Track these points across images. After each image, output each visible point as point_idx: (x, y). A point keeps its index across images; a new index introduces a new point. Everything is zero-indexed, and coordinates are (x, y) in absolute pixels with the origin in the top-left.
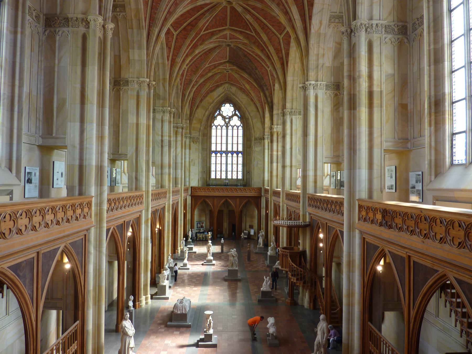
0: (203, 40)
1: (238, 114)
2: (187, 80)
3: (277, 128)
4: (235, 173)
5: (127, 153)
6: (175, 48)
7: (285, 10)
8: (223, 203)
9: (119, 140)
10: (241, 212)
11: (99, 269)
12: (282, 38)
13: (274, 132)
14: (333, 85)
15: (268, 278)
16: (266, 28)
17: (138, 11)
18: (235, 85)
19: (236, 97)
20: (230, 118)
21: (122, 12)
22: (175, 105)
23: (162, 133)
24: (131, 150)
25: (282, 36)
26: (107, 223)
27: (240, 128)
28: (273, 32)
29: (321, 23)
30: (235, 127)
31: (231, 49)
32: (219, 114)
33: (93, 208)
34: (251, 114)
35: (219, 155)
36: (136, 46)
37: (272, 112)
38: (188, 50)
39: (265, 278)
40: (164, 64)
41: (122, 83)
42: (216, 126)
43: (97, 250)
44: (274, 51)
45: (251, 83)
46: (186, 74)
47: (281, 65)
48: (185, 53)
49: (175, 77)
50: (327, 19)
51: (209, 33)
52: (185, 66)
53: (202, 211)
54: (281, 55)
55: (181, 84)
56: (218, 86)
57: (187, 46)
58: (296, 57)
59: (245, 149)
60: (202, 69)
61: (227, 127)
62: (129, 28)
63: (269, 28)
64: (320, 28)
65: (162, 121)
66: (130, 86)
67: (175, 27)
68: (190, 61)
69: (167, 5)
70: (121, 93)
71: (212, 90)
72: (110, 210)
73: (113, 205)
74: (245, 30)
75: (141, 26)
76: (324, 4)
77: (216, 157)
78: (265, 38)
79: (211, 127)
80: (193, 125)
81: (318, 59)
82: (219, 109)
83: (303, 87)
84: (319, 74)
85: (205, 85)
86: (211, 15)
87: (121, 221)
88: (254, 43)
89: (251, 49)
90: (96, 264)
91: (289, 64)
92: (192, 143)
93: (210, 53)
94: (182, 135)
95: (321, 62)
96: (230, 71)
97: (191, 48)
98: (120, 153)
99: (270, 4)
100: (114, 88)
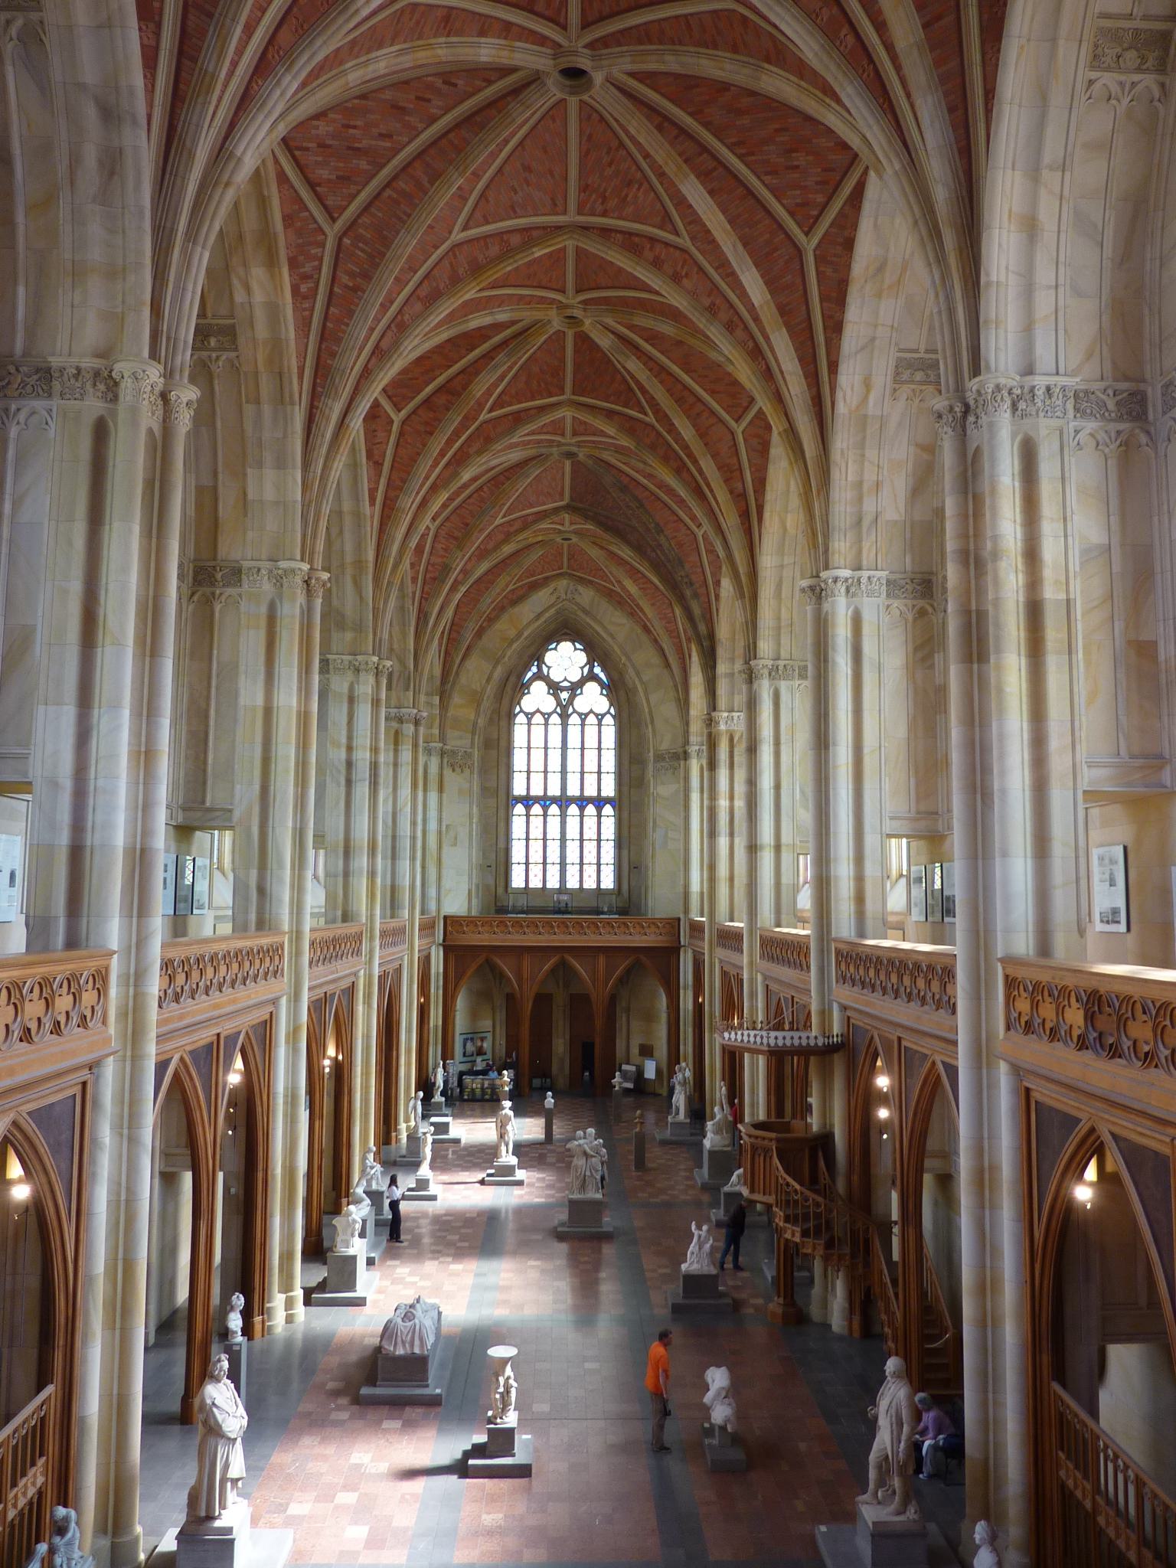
0: (485, 438)
1: (602, 676)
2: (433, 565)
3: (733, 722)
4: (590, 871)
5: (231, 804)
6: (396, 465)
7: (751, 344)
8: (553, 971)
9: (205, 762)
10: (613, 999)
11: (127, 1201)
13: (719, 734)
14: (912, 580)
15: (705, 1228)
17: (276, 345)
18: (591, 582)
19: (594, 618)
20: (575, 688)
21: (225, 350)
22: (396, 646)
23: (350, 738)
24: (244, 795)
25: (744, 424)
26: (158, 1043)
27: (609, 720)
28: (713, 413)
29: (867, 384)
30: (591, 716)
31: (577, 467)
32: (539, 676)
33: (113, 991)
35: (537, 809)
36: (268, 457)
37: (714, 667)
38: (438, 470)
39: (693, 1227)
40: (357, 515)
41: (219, 576)
42: (526, 714)
43: (121, 1135)
45: (644, 576)
48: (427, 478)
50: (889, 373)
51: (505, 416)
52: (426, 521)
53: (482, 998)
54: (739, 485)
55: (414, 580)
56: (534, 587)
58: (788, 491)
59: (625, 789)
60: (482, 530)
61: (564, 717)
62: (247, 402)
63: (699, 400)
64: (866, 398)
65: (351, 700)
66: (245, 586)
68: (444, 506)
69: (372, 330)
70: (218, 608)
71: (516, 599)
72: (172, 996)
73: (180, 979)
74: (626, 406)
75: (287, 395)
76: (876, 326)
77: (528, 816)
78: (687, 432)
79: (511, 717)
81: (860, 499)
82: (538, 660)
83: (812, 588)
84: (866, 545)
85: (492, 582)
86: (513, 360)
87: (206, 1036)
88: (653, 447)
89: (641, 466)
90: (120, 1184)
91: (767, 515)
92: (447, 772)
93: (508, 479)
94: (415, 746)
95: (869, 506)
96: (575, 539)
98: (208, 804)
99: (701, 326)
100: (193, 594)
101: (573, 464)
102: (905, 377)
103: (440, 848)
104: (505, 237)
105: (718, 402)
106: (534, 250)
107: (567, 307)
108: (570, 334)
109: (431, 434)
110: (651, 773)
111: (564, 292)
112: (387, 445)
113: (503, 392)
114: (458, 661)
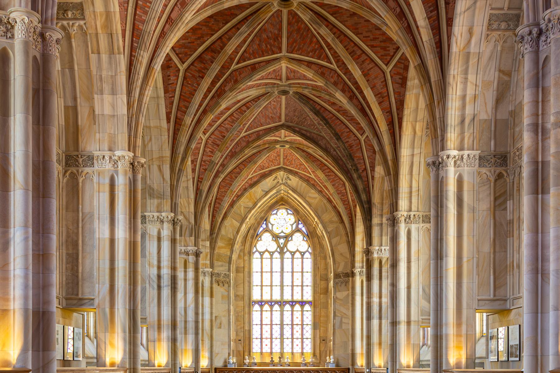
6: (182, 97)
12: (390, 72)
13: (373, 259)
16: (359, 52)
27: (307, 255)
28: (372, 60)
34: (328, 228)
37: (370, 220)
38: (207, 101)
44: (374, 99)
46: (204, 151)
47: (388, 125)
49: (183, 155)
50: (485, 24)
52: (200, 134)
58: (417, 108)
61: (282, 253)
63: (364, 52)
68: (210, 125)
80: (216, 251)
86: (251, 30)
88: (335, 84)
89: (327, 97)
91: (404, 124)
94: (197, 269)
97: (213, 97)
101: (286, 98)
102: (495, 26)
103: (212, 329)
105: (374, 53)
108: (285, 12)
109: (203, 78)
110: (332, 285)
112: (177, 84)
113: (245, 51)
114: (220, 220)
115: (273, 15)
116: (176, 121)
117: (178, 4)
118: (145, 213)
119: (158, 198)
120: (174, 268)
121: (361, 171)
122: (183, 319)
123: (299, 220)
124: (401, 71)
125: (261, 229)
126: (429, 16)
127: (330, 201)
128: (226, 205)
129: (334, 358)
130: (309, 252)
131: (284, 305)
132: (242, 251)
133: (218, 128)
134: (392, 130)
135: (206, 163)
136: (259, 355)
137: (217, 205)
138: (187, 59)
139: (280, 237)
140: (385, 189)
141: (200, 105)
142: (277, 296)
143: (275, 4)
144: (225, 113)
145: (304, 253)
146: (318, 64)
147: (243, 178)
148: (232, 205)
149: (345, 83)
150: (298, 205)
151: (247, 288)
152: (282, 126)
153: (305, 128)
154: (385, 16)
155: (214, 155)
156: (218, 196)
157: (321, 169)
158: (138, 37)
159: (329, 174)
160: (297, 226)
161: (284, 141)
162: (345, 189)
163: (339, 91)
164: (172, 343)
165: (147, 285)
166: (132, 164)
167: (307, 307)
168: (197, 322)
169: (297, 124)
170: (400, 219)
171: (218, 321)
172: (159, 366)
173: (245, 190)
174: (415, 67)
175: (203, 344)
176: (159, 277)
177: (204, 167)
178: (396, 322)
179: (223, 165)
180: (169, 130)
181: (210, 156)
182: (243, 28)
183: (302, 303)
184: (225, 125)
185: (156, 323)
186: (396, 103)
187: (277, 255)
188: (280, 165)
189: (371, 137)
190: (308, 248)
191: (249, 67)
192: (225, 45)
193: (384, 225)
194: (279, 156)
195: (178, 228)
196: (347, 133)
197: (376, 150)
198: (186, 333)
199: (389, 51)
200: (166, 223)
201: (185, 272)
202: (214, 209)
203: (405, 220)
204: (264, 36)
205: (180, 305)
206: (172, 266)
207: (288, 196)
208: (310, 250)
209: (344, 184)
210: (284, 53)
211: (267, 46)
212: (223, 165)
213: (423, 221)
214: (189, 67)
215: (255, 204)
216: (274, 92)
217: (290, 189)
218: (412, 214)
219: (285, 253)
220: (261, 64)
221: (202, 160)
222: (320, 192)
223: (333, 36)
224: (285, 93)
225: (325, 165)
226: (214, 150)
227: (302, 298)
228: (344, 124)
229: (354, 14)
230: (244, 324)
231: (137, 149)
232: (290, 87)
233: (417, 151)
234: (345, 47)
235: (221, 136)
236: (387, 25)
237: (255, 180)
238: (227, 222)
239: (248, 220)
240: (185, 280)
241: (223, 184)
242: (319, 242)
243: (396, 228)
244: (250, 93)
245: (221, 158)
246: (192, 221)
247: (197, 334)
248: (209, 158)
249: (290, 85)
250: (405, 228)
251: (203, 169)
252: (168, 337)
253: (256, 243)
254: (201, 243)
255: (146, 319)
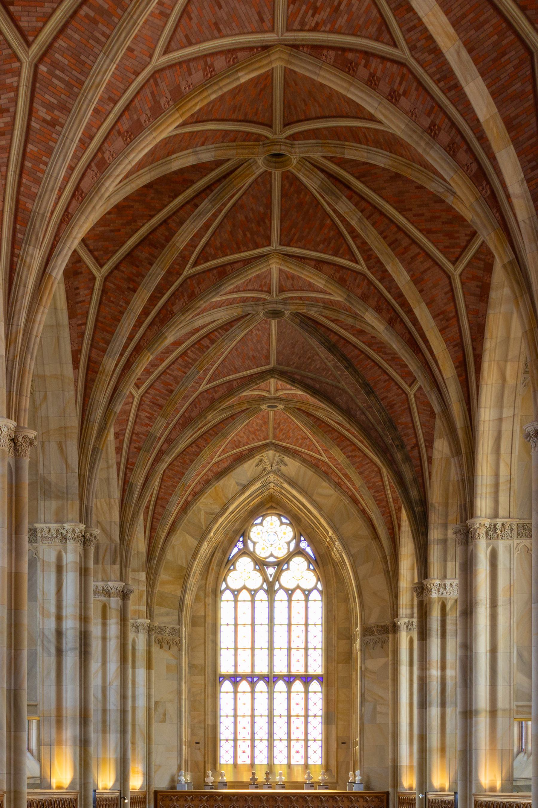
6: (99, 324)
12: (460, 275)
13: (430, 602)
27: (315, 595)
28: (428, 256)
34: (351, 549)
37: (426, 534)
44: (433, 323)
46: (137, 416)
47: (456, 368)
49: (100, 424)
52: (130, 388)
57: (139, 318)
58: (508, 337)
61: (271, 592)
63: (414, 242)
67: (97, 250)
68: (148, 372)
80: (158, 589)
86: (217, 207)
88: (364, 298)
89: (350, 321)
91: (486, 365)
97: (152, 324)
99: (420, 151)
104: (209, 60)
105: (433, 243)
106: (240, 74)
107: (274, 143)
108: (277, 174)
109: (134, 291)
110: (358, 647)
111: (270, 126)
112: (90, 303)
113: (207, 244)
114: (163, 536)
115: (256, 180)
116: (88, 365)
117: (93, 164)
118: (35, 525)
119: (58, 497)
120: (84, 619)
121: (408, 448)
122: (100, 707)
123: (301, 535)
124: (480, 273)
125: (235, 550)
126: (529, 176)
127: (354, 501)
128: (174, 509)
129: (362, 774)
130: (318, 590)
131: (275, 682)
132: (202, 588)
133: (162, 377)
134: (464, 377)
135: (141, 438)
136: (230, 768)
137: (159, 509)
138: (108, 260)
139: (268, 565)
140: (452, 479)
141: (130, 338)
142: (262, 668)
143: (260, 162)
144: (173, 352)
145: (310, 591)
146: (335, 265)
147: (204, 462)
148: (185, 508)
149: (382, 296)
150: (299, 508)
151: (209, 652)
152: (271, 372)
153: (311, 375)
154: (452, 178)
155: (154, 422)
156: (161, 494)
157: (338, 446)
158: (25, 223)
159: (353, 454)
160: (297, 545)
161: (275, 398)
162: (382, 480)
163: (370, 310)
164: (80, 747)
165: (39, 649)
166: (14, 440)
167: (315, 686)
168: (123, 712)
169: (297, 368)
170: (478, 531)
171: (161, 710)
172: (59, 788)
173: (207, 483)
174: (504, 266)
175: (134, 749)
176: (59, 634)
177: (137, 445)
178: (471, 712)
179: (169, 441)
180: (76, 381)
181: (147, 425)
182: (205, 204)
183: (306, 679)
184: (173, 371)
185: (54, 713)
186: (471, 329)
187: (262, 595)
188: (268, 439)
189: (427, 389)
190: (317, 583)
191: (215, 272)
192: (172, 234)
193: (449, 542)
194: (266, 423)
195: (92, 550)
196: (385, 382)
197: (436, 412)
198: (104, 731)
199: (458, 238)
200: (72, 540)
201: (104, 625)
202: (153, 517)
203: (487, 533)
204: (241, 217)
205: (95, 681)
206: (80, 615)
207: (282, 494)
208: (320, 586)
209: (380, 471)
210: (275, 245)
211: (245, 235)
212: (169, 441)
213: (519, 536)
214: (111, 272)
215: (225, 508)
216: (257, 314)
217: (285, 480)
218: (499, 522)
219: (276, 592)
220: (236, 265)
221: (133, 433)
222: (338, 485)
223: (360, 214)
224: (276, 314)
225: (347, 439)
226: (153, 415)
227: (306, 670)
228: (380, 368)
229: (397, 176)
230: (205, 714)
231: (22, 414)
232: (285, 304)
233: (507, 412)
234: (381, 233)
235: (167, 390)
236: (454, 194)
237: (225, 465)
238: (177, 539)
239: (212, 534)
240: (104, 639)
241: (168, 473)
242: (336, 573)
243: (470, 548)
244: (216, 316)
245: (166, 428)
246: (117, 538)
247: (123, 732)
248: (145, 429)
249: (285, 301)
250: (487, 547)
251: (135, 448)
252: (74, 737)
253: (227, 575)
254: (131, 575)
255: (36, 706)
